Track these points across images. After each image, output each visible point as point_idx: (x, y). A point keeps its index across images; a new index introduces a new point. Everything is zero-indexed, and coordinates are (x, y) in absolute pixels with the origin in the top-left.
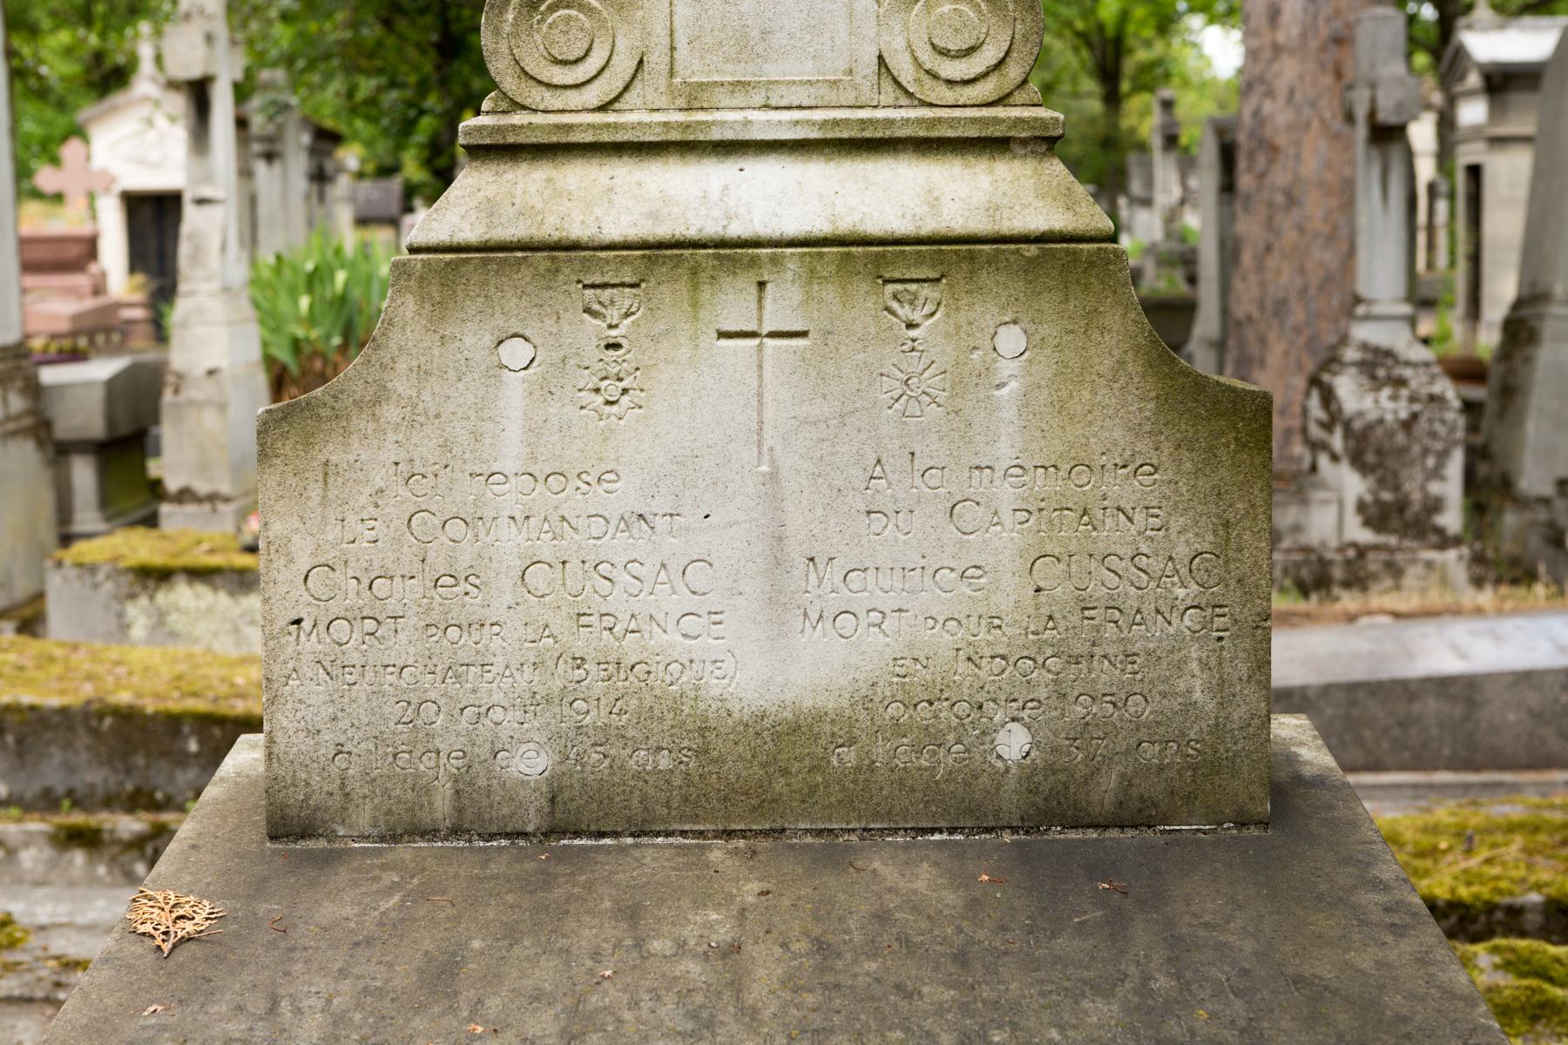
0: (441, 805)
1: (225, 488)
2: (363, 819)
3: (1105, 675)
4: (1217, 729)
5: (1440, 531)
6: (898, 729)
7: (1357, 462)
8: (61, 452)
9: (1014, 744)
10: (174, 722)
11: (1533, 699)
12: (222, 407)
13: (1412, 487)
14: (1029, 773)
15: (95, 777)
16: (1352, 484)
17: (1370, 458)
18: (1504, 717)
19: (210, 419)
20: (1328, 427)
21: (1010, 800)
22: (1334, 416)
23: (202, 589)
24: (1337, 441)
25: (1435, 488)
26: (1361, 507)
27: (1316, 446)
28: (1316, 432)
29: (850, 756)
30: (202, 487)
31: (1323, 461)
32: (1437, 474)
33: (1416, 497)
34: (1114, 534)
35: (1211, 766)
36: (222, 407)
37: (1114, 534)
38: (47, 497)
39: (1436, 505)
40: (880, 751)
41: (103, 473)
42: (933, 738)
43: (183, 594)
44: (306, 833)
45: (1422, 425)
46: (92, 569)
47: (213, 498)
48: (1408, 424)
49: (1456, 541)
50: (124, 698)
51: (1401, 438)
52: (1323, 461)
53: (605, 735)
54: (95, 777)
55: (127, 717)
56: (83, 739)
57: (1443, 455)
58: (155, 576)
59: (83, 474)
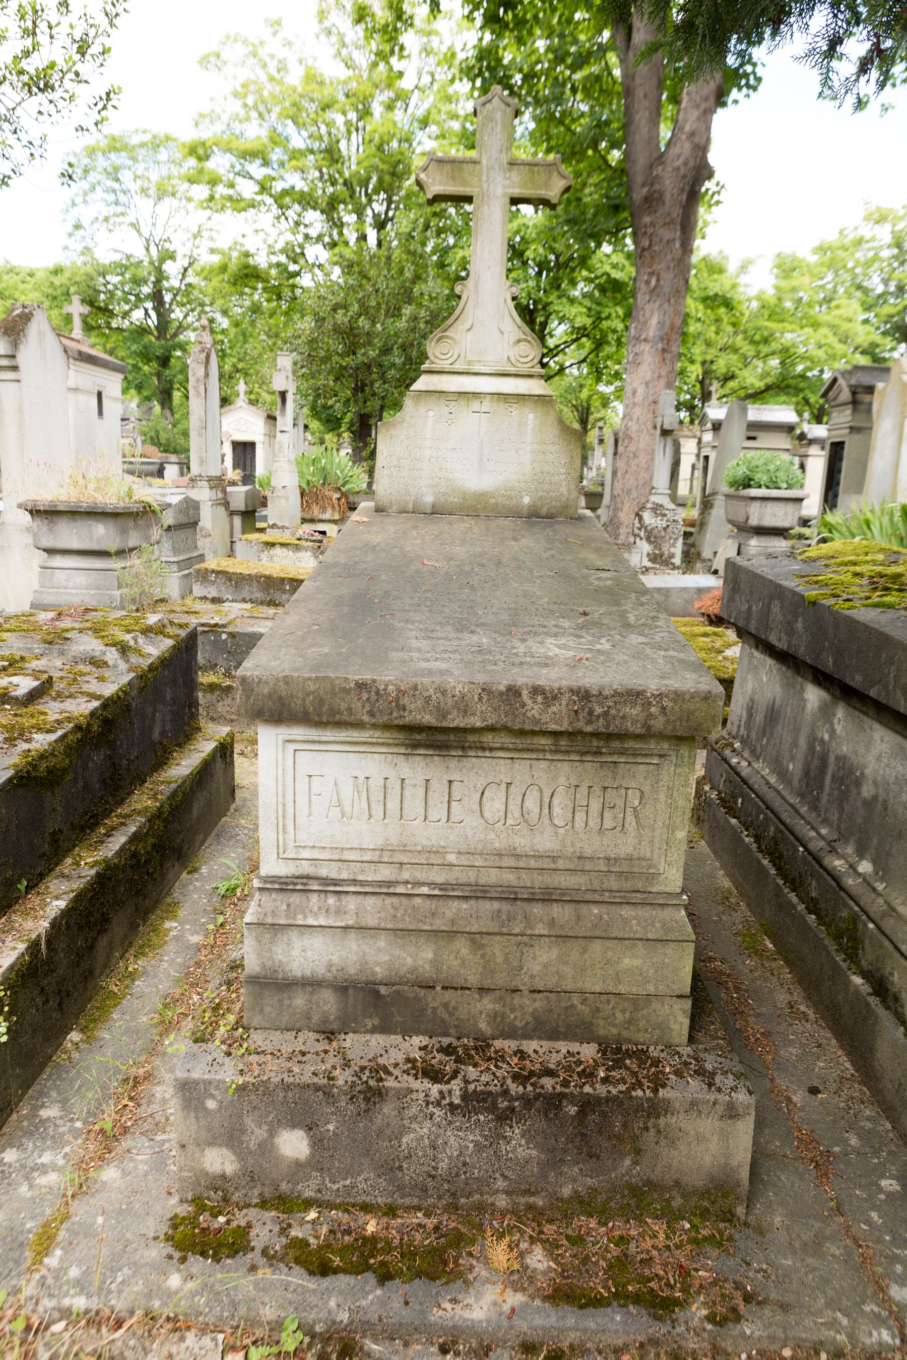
0: (410, 507)
1: (287, 525)
2: (394, 509)
3: (546, 487)
4: (568, 499)
5: (673, 564)
6: (503, 496)
7: (648, 539)
8: (232, 513)
9: (526, 500)
10: (282, 580)
11: (686, 596)
12: (287, 498)
13: (665, 549)
14: (529, 506)
15: (259, 595)
16: (645, 547)
17: (652, 539)
18: (677, 601)
19: (283, 502)
20: (640, 529)
21: (525, 512)
22: (642, 526)
23: (284, 550)
24: (642, 534)
25: (672, 550)
26: (648, 555)
27: (635, 536)
28: (636, 531)
29: (493, 501)
30: (280, 524)
31: (638, 540)
32: (673, 545)
33: (666, 552)
34: (550, 458)
35: (566, 507)
36: (287, 498)
37: (550, 458)
38: (228, 526)
39: (672, 556)
40: (499, 500)
41: (243, 521)
42: (510, 498)
43: (278, 550)
44: (382, 511)
45: (670, 528)
46: (251, 542)
47: (283, 527)
48: (665, 529)
49: (678, 568)
50: (267, 573)
51: (663, 533)
52: (638, 540)
53: (444, 494)
54: (259, 595)
55: (268, 578)
56: (255, 584)
57: (676, 539)
58: (271, 545)
59: (237, 521)
